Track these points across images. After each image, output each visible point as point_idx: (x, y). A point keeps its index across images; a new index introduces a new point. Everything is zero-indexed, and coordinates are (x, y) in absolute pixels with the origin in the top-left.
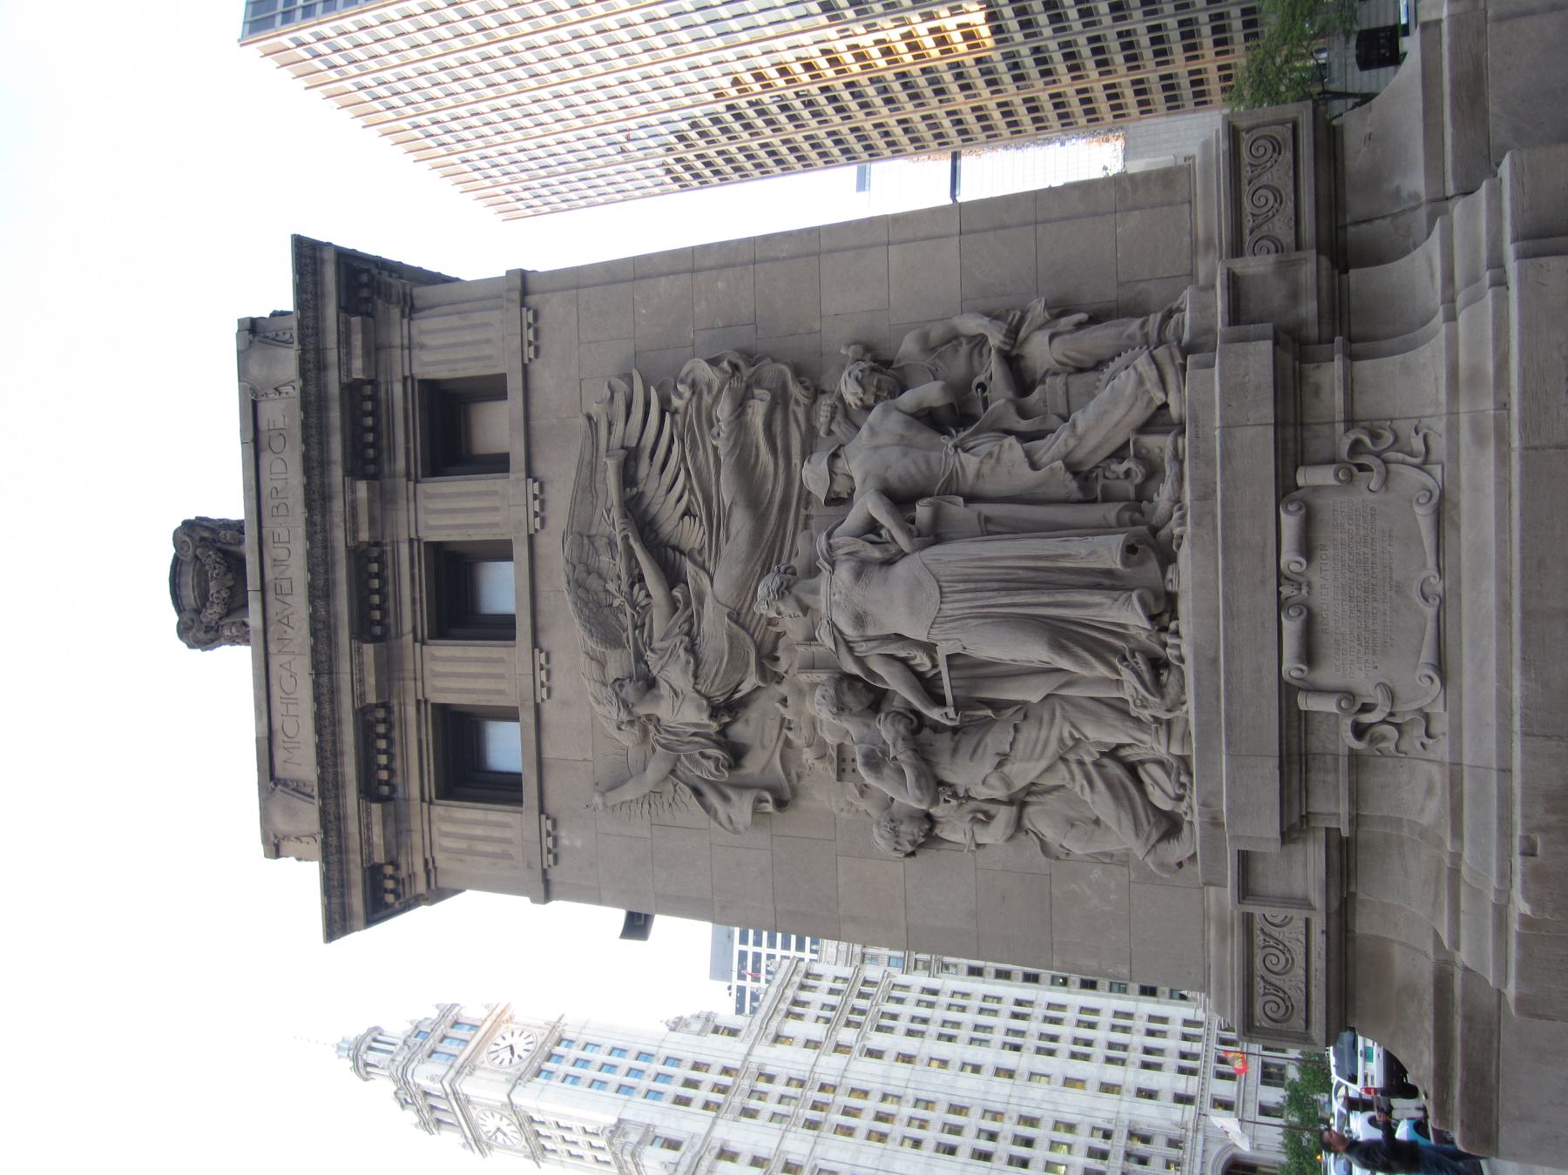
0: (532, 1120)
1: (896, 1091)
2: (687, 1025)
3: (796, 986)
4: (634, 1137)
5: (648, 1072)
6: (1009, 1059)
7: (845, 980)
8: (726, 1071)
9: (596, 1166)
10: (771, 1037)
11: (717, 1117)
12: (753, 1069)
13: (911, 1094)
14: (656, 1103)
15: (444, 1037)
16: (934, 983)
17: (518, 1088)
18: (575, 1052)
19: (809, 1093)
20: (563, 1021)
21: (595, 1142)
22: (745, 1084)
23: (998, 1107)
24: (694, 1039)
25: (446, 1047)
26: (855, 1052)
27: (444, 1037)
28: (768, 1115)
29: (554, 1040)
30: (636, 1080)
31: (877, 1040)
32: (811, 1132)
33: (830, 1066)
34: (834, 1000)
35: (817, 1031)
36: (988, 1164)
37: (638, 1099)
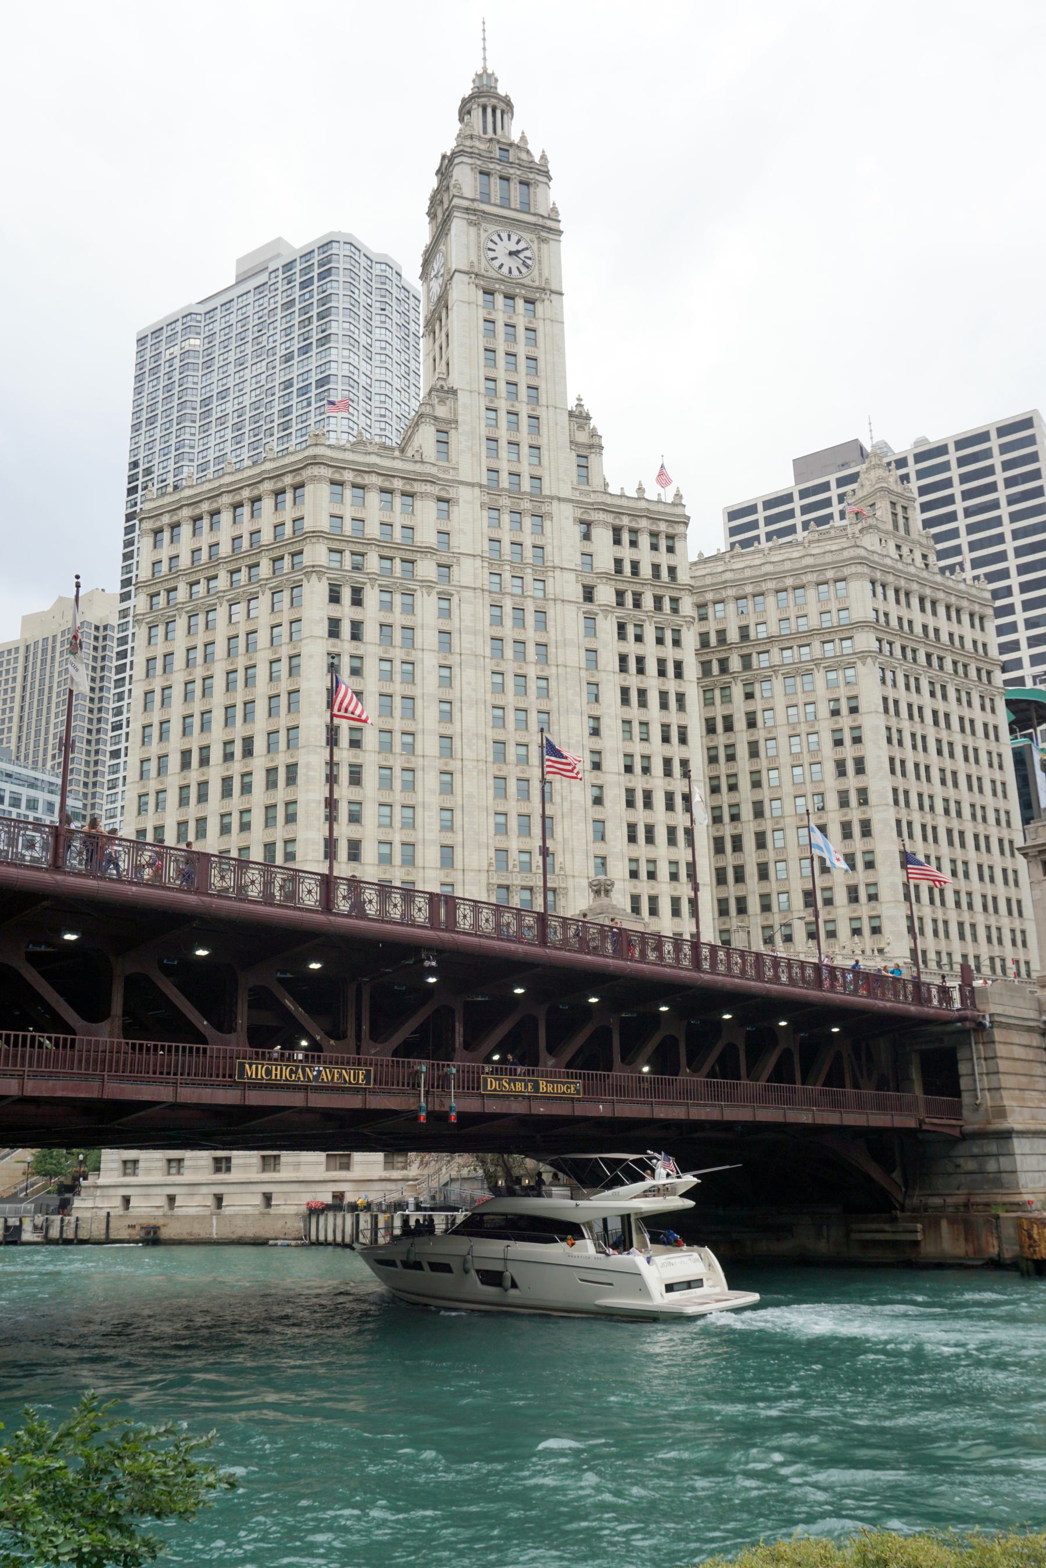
1: (551, 657)
2: (581, 427)
3: (654, 528)
4: (441, 411)
5: (516, 404)
10: (585, 517)
12: (545, 508)
15: (505, 179)
17: (465, 278)
18: (521, 322)
19: (529, 571)
20: (554, 297)
24: (565, 439)
26: (588, 606)
27: (505, 179)
29: (530, 295)
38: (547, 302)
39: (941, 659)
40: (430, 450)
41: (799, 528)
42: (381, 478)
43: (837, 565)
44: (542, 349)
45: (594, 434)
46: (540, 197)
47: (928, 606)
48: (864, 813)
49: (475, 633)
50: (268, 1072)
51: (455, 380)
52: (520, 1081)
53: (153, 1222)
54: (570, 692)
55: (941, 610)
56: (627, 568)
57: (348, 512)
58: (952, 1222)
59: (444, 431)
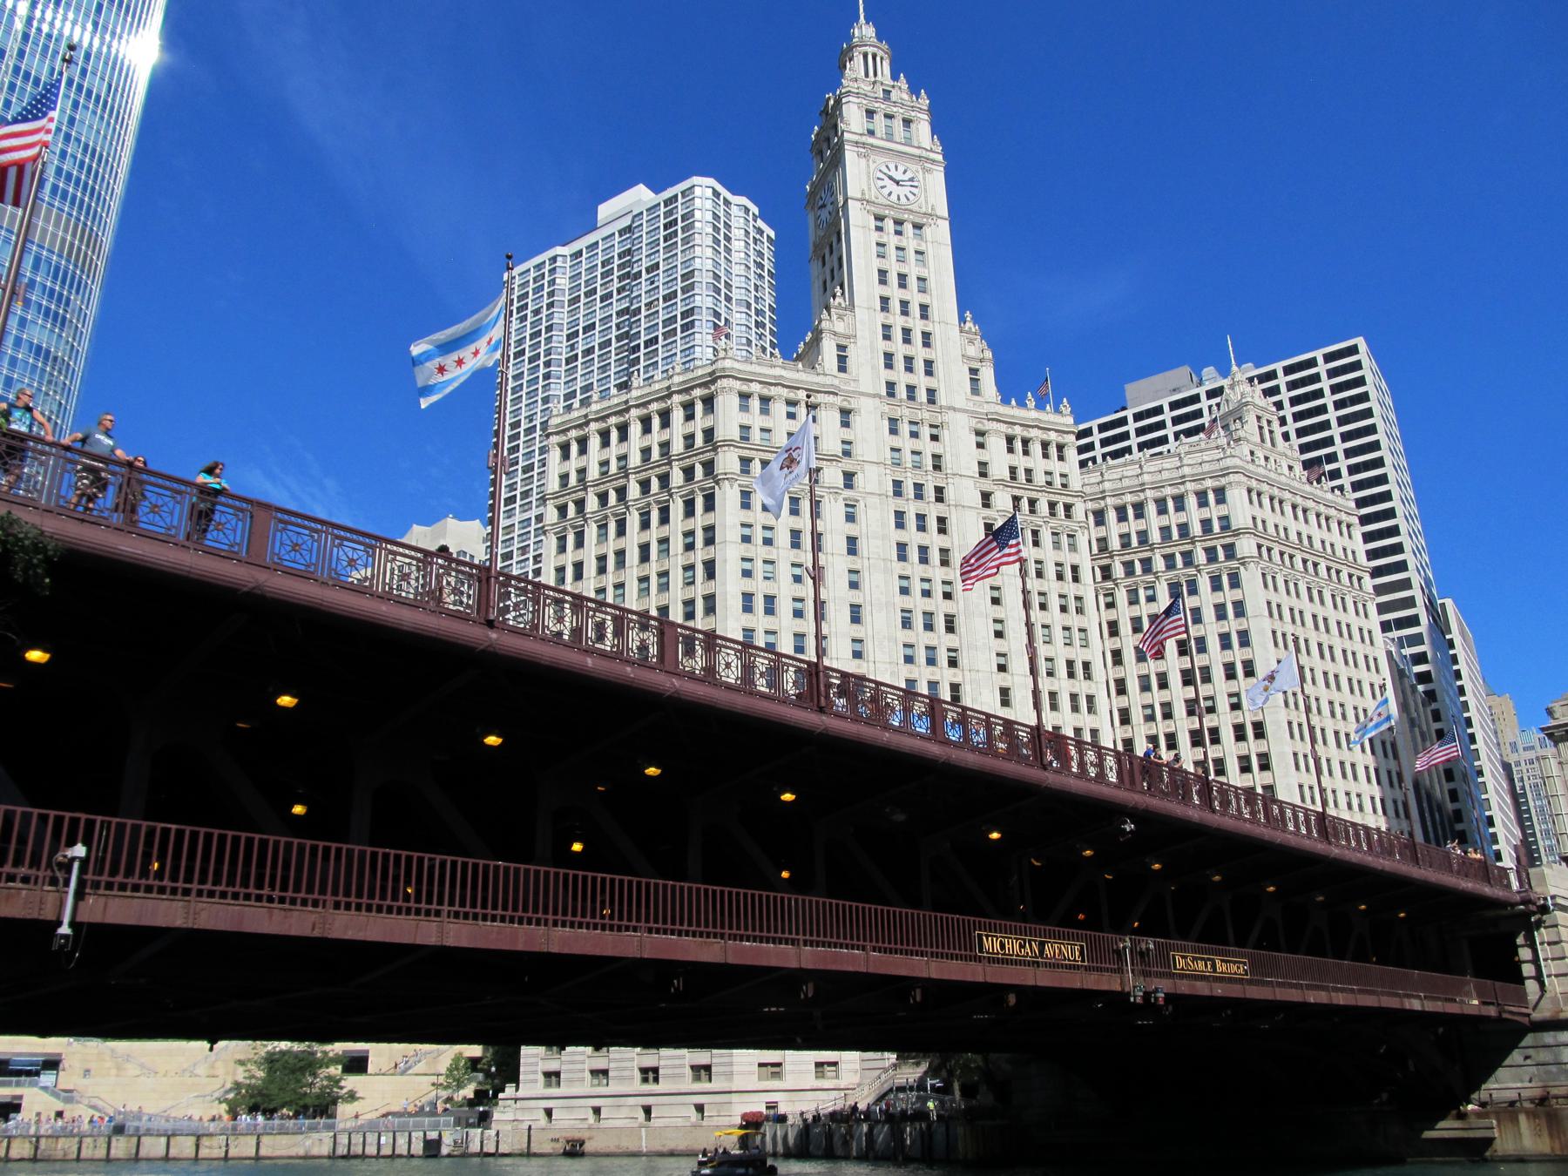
8: (931, 393)
10: (980, 427)
15: (889, 117)
16: (1086, 574)
17: (859, 203)
26: (987, 512)
27: (889, 117)
35: (999, 470)
39: (1315, 565)
41: (1171, 438)
44: (932, 269)
47: (1300, 514)
50: (1002, 946)
52: (1202, 959)
53: (577, 1135)
55: (1312, 518)
56: (1022, 476)
58: (1531, 1114)
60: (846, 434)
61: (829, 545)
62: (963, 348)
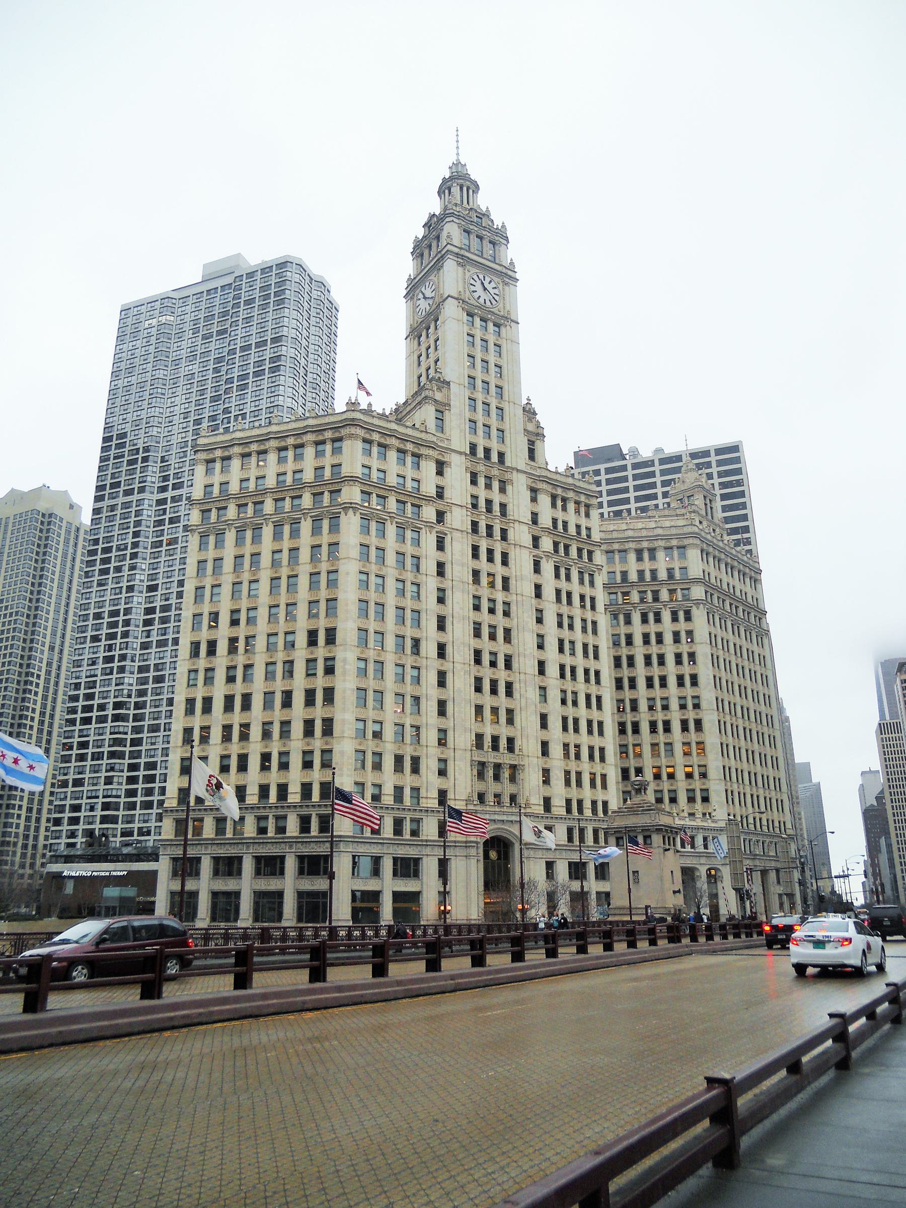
0: (436, 320)
2: (530, 420)
4: (438, 396)
5: (488, 397)
6: (552, 670)
7: (589, 536)
8: (501, 455)
9: (416, 378)
10: (533, 485)
11: (466, 455)
12: (507, 476)
13: (512, 598)
14: (467, 407)
16: (600, 606)
17: (456, 302)
18: (492, 339)
21: (431, 371)
22: (495, 472)
23: (515, 665)
24: (520, 428)
25: (475, 242)
26: (536, 552)
27: (480, 238)
28: (475, 493)
29: (498, 321)
30: (481, 390)
31: (548, 567)
32: (470, 527)
33: (521, 534)
34: (572, 530)
35: (545, 521)
36: (472, 662)
37: (467, 393)
38: (508, 327)
40: (431, 425)
42: (398, 441)
43: (680, 537)
45: (538, 426)
46: (502, 254)
48: (697, 714)
49: (463, 565)
51: (448, 375)
54: (526, 615)
57: (375, 464)
59: (441, 410)
60: (440, 481)
61: (424, 567)
62: (525, 424)
